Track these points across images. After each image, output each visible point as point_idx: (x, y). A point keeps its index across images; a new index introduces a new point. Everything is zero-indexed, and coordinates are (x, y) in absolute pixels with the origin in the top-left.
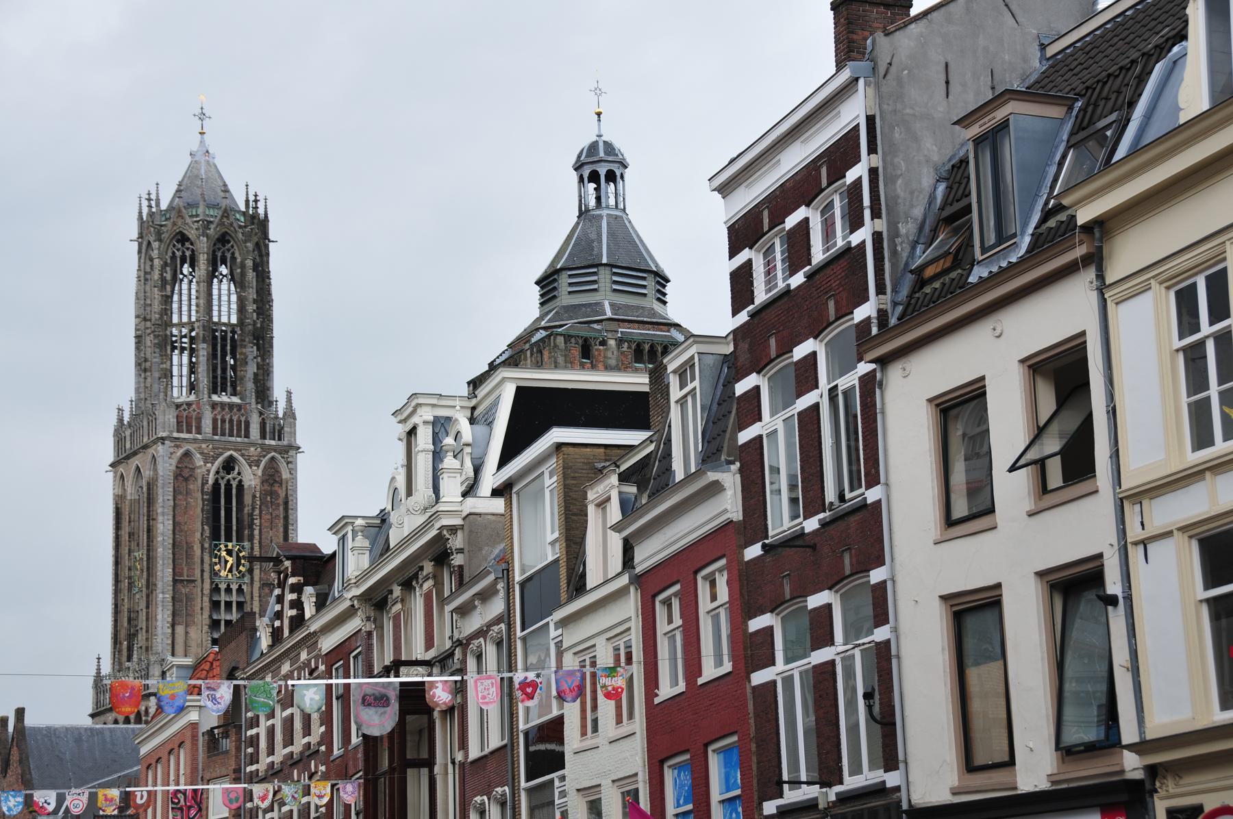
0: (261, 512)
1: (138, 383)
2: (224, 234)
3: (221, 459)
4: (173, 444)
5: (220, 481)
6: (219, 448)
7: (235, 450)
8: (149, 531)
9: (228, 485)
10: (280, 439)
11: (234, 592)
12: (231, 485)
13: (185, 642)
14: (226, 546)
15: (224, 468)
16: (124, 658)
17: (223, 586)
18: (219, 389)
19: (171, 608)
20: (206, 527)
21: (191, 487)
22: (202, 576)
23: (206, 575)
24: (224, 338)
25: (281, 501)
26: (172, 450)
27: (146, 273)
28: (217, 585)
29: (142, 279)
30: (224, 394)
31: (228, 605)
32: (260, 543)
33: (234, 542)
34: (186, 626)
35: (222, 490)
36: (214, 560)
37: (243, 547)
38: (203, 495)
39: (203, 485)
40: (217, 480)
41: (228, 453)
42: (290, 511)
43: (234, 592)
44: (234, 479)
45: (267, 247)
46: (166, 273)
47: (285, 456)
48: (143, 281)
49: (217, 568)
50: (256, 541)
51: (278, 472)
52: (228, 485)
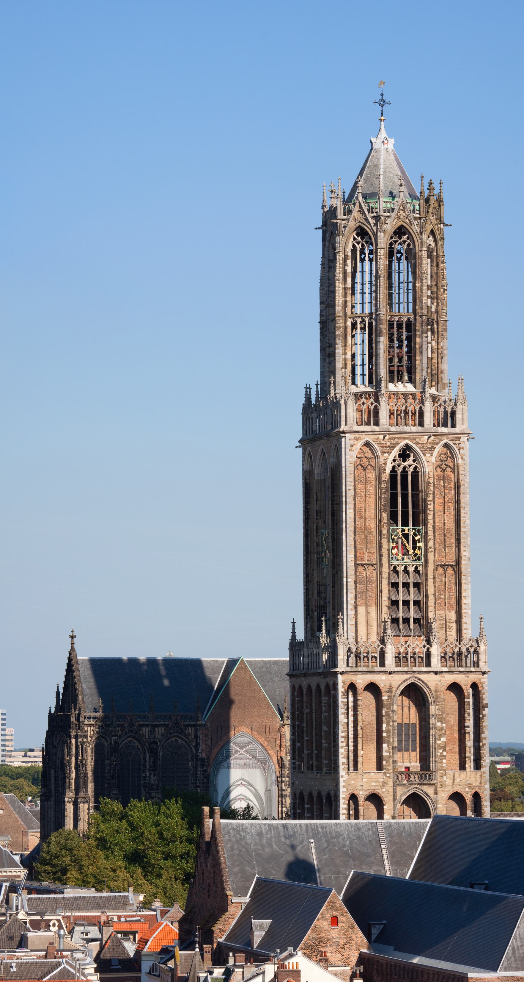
0: (434, 498)
1: (322, 367)
2: (401, 228)
4: (353, 437)
6: (395, 438)
7: (410, 439)
8: (333, 515)
9: (404, 471)
10: (453, 425)
14: (403, 531)
15: (400, 456)
16: (316, 628)
17: (401, 569)
18: (396, 378)
20: (384, 514)
24: (400, 325)
25: (452, 485)
26: (352, 442)
27: (330, 261)
28: (395, 567)
29: (326, 266)
30: (400, 383)
31: (406, 585)
32: (434, 527)
33: (411, 526)
34: (367, 607)
35: (399, 478)
36: (391, 544)
37: (419, 531)
40: (394, 467)
41: (403, 443)
44: (410, 466)
45: (441, 231)
47: (457, 442)
48: (327, 269)
49: (394, 551)
50: (430, 526)
52: (404, 471)
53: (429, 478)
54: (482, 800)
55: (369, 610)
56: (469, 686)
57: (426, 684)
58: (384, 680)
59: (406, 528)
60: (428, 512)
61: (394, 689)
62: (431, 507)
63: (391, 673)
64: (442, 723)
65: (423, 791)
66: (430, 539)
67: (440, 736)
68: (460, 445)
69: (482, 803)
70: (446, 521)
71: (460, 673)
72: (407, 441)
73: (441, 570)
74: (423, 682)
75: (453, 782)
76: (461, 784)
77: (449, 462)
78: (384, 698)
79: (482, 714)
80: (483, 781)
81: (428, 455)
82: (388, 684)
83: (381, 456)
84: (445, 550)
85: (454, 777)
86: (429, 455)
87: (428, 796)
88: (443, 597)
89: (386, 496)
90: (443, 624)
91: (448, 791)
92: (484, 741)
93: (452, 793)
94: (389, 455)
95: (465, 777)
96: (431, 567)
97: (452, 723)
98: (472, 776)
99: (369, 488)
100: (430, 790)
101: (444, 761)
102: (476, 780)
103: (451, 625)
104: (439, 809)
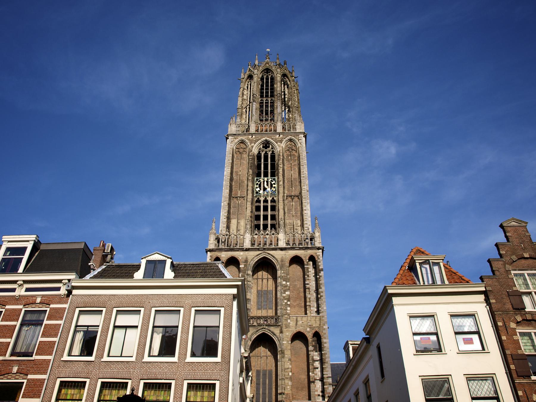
3: (260, 141)
4: (233, 138)
6: (259, 137)
7: (268, 137)
11: (269, 202)
13: (237, 227)
17: (262, 199)
20: (250, 170)
21: (244, 156)
23: (250, 192)
25: (296, 158)
26: (232, 140)
36: (256, 186)
37: (274, 179)
38: (249, 156)
39: (249, 152)
40: (259, 152)
41: (264, 139)
42: (301, 160)
43: (269, 202)
44: (269, 151)
47: (297, 137)
51: (295, 145)
53: (280, 153)
54: (322, 337)
55: (239, 221)
56: (307, 258)
57: (274, 257)
58: (241, 255)
59: (266, 179)
60: (279, 168)
61: (249, 260)
63: (247, 250)
64: (286, 282)
65: (270, 331)
66: (280, 181)
67: (285, 291)
68: (299, 138)
69: (322, 340)
70: (293, 175)
71: (300, 249)
72: (266, 138)
73: (290, 199)
74: (272, 255)
75: (296, 324)
76: (303, 325)
77: (294, 148)
78: (240, 266)
79: (319, 275)
80: (321, 323)
81: (278, 143)
82: (245, 257)
83: (249, 145)
84: (292, 188)
85: (297, 320)
86: (280, 143)
87: (275, 335)
88: (292, 213)
89: (252, 162)
90: (291, 228)
91: (291, 331)
92: (322, 294)
93: (295, 332)
94: (255, 144)
95: (306, 320)
96: (281, 195)
97: (298, 286)
98: (312, 320)
99: (243, 161)
100: (276, 331)
101: (289, 308)
102: (316, 323)
103: (297, 228)
104: (284, 345)
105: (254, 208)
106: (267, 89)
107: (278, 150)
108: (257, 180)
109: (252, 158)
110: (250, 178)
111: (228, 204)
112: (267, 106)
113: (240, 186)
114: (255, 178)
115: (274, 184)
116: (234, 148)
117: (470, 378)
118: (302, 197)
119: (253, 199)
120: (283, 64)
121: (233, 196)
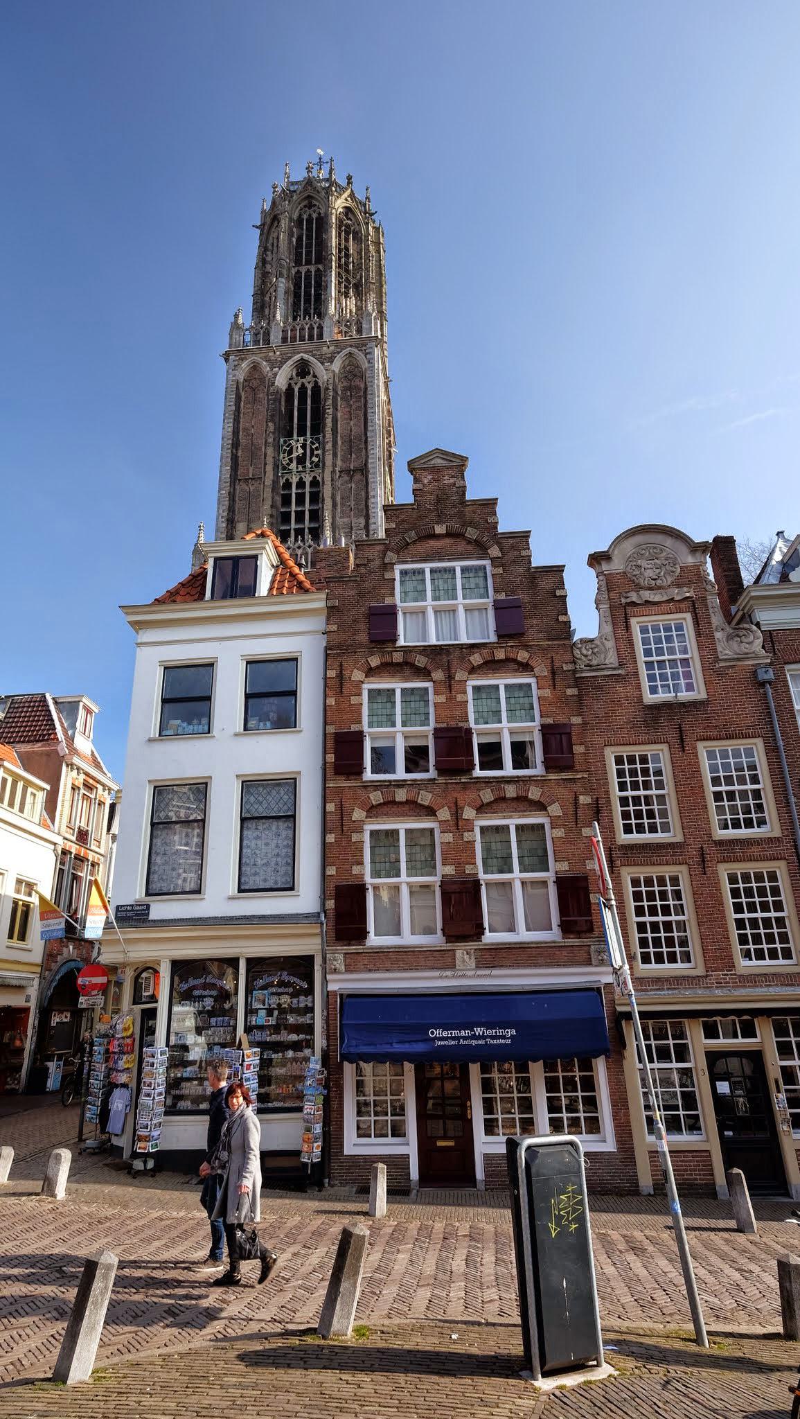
3: (290, 362)
5: (293, 385)
7: (305, 352)
9: (303, 389)
12: (306, 388)
17: (294, 480)
19: (227, 503)
20: (270, 424)
21: (261, 395)
22: (265, 469)
23: (269, 468)
25: (362, 393)
26: (236, 363)
34: (249, 522)
37: (317, 439)
38: (268, 395)
40: (290, 385)
41: (297, 357)
42: (369, 396)
44: (309, 383)
46: (267, 256)
47: (363, 348)
52: (303, 389)
59: (302, 439)
60: (326, 416)
62: (330, 411)
70: (353, 429)
73: (346, 478)
105: (279, 500)
106: (309, 245)
107: (325, 377)
108: (285, 442)
109: (274, 400)
110: (270, 440)
111: (229, 493)
112: (308, 286)
113: (253, 454)
114: (282, 440)
115: (317, 449)
116: (242, 380)
117: (249, 785)
118: (367, 472)
119: (275, 482)
120: (343, 183)
121: (239, 478)
